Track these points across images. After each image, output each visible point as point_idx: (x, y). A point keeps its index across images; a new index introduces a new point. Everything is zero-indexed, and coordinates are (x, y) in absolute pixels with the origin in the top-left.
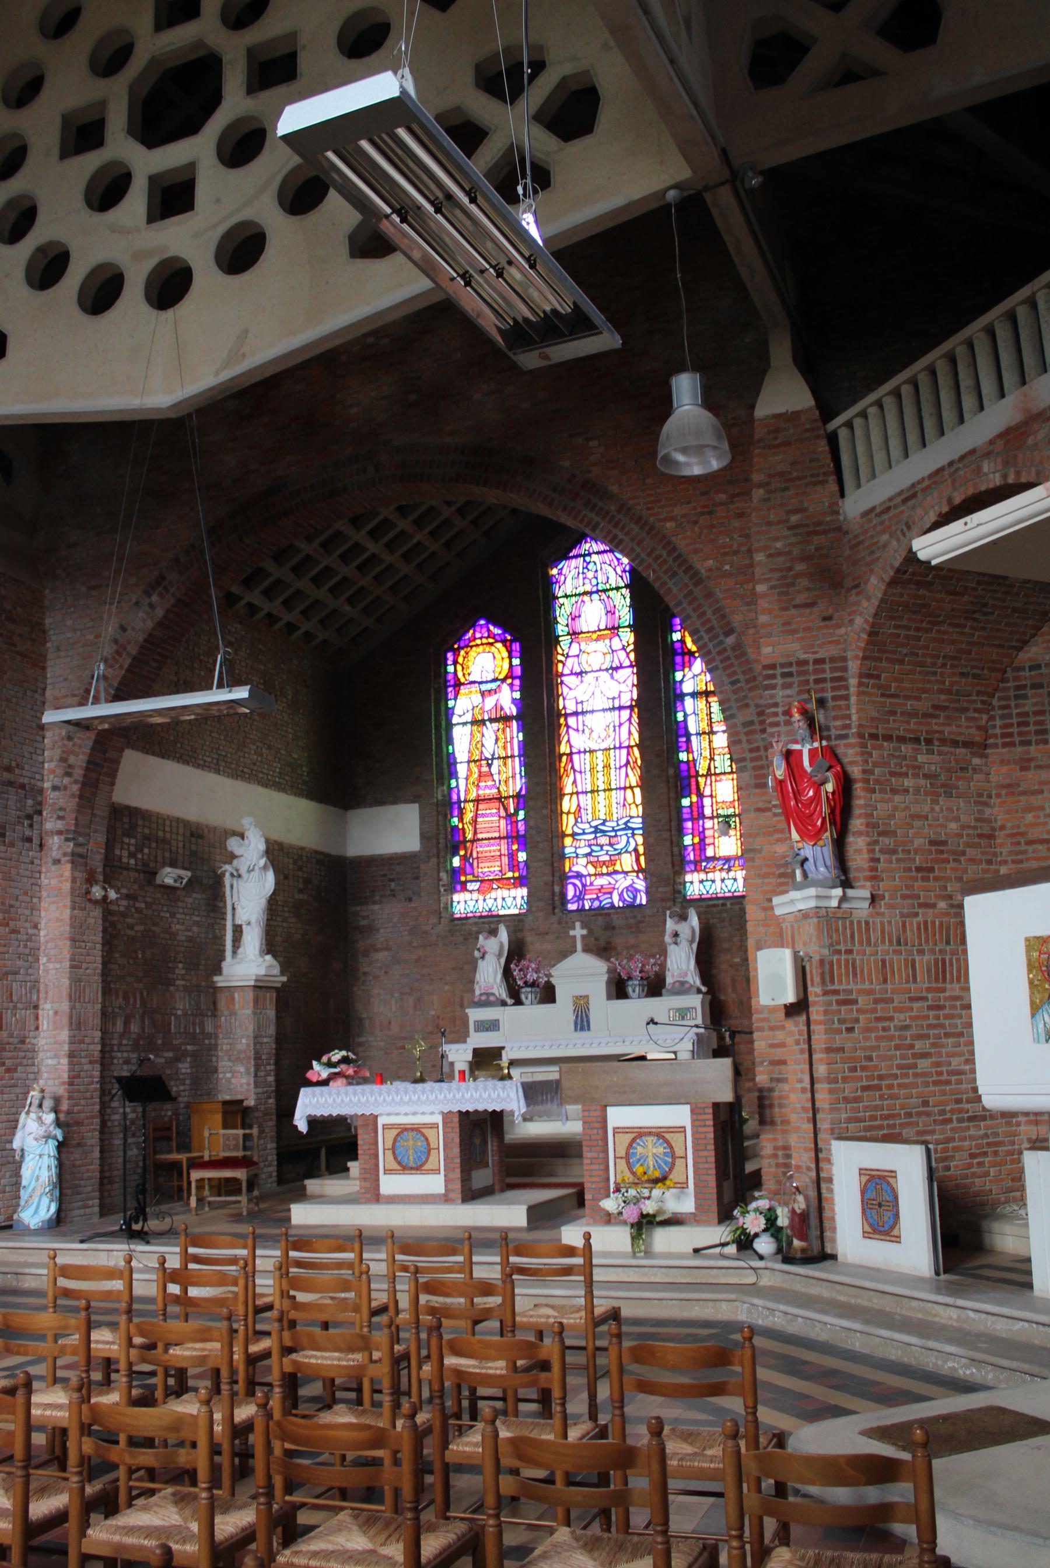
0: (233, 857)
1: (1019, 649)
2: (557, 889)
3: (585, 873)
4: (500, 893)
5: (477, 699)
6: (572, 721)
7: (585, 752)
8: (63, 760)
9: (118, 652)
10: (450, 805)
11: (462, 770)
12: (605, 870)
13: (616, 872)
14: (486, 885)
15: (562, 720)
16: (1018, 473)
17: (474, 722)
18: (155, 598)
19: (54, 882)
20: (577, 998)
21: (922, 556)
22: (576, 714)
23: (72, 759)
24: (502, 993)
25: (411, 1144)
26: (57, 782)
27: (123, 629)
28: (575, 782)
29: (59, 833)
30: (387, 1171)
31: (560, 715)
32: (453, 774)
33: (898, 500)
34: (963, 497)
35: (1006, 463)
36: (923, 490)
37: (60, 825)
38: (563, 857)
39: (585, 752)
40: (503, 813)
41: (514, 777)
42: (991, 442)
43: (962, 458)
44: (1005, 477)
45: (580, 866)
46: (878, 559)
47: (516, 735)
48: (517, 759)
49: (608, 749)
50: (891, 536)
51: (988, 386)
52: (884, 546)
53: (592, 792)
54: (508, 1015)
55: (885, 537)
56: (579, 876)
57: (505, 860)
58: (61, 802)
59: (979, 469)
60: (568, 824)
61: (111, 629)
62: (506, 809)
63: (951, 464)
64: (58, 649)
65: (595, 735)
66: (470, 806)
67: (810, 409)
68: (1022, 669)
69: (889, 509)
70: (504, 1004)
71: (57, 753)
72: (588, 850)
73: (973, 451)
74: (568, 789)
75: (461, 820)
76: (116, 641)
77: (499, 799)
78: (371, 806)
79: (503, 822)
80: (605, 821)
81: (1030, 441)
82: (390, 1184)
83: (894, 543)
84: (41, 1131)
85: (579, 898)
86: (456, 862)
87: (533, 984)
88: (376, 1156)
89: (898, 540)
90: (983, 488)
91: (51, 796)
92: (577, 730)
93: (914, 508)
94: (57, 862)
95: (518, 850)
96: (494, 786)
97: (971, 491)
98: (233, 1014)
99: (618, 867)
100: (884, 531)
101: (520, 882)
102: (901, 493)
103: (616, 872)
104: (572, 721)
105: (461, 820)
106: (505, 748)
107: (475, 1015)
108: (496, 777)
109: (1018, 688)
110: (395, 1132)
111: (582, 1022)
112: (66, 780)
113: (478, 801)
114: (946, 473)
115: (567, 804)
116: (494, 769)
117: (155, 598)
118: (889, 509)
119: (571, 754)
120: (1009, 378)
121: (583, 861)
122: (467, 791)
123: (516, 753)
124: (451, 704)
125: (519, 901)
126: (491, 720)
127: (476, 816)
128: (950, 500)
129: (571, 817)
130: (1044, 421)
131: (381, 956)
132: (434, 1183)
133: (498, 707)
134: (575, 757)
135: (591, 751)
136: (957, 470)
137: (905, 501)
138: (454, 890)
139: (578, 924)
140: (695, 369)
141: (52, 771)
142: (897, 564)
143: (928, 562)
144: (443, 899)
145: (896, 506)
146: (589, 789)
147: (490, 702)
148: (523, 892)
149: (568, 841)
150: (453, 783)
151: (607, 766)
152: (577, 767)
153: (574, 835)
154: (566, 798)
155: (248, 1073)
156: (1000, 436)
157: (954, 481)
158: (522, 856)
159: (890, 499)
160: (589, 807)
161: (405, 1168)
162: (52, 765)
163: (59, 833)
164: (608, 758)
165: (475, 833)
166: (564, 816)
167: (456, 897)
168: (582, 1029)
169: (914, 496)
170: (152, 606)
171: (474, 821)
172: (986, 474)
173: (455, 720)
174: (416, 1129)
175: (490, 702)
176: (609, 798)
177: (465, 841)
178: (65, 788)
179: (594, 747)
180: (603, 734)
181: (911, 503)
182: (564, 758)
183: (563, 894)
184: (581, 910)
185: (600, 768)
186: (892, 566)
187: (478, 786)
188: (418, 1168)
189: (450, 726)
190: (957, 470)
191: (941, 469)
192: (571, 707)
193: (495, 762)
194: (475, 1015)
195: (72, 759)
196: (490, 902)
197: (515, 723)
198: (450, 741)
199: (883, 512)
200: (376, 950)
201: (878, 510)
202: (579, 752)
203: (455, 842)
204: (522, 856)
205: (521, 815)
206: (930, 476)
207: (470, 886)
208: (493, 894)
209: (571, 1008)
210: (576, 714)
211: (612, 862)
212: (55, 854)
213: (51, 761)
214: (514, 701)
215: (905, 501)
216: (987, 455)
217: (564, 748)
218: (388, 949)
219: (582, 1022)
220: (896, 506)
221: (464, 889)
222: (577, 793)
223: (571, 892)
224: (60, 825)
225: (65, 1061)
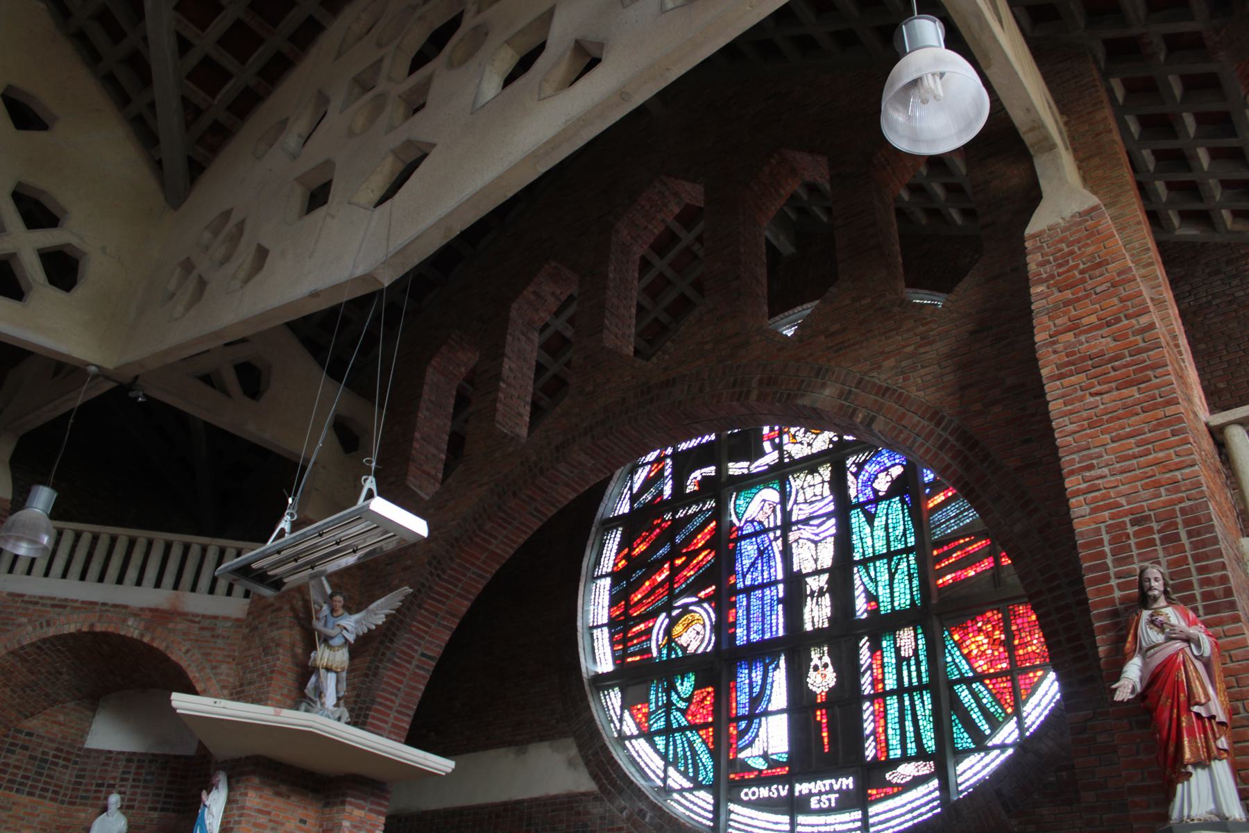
1: (27, 717)
16: (153, 639)
21: (174, 704)
33: (49, 602)
34: (103, 630)
35: (147, 628)
36: (73, 608)
42: (142, 609)
43: (115, 606)
44: (142, 635)
46: (8, 631)
50: (29, 621)
51: (151, 573)
52: (20, 625)
55: (24, 620)
59: (125, 620)
63: (104, 604)
67: (7, 500)
68: (20, 731)
69: (36, 603)
73: (126, 607)
81: (171, 626)
83: (30, 628)
89: (35, 628)
90: (122, 633)
93: (59, 614)
97: (111, 629)
100: (25, 615)
102: (54, 599)
109: (12, 744)
114: (98, 608)
118: (36, 603)
120: (169, 579)
128: (92, 625)
130: (184, 620)
136: (107, 611)
137: (54, 606)
140: (54, 487)
142: (25, 643)
143: (174, 710)
145: (43, 605)
156: (151, 610)
157: (101, 616)
159: (42, 598)
169: (64, 607)
172: (128, 626)
181: (57, 610)
186: (19, 642)
190: (107, 611)
191: (94, 603)
199: (30, 602)
201: (26, 599)
206: (83, 602)
215: (54, 606)
216: (135, 615)
220: (43, 605)
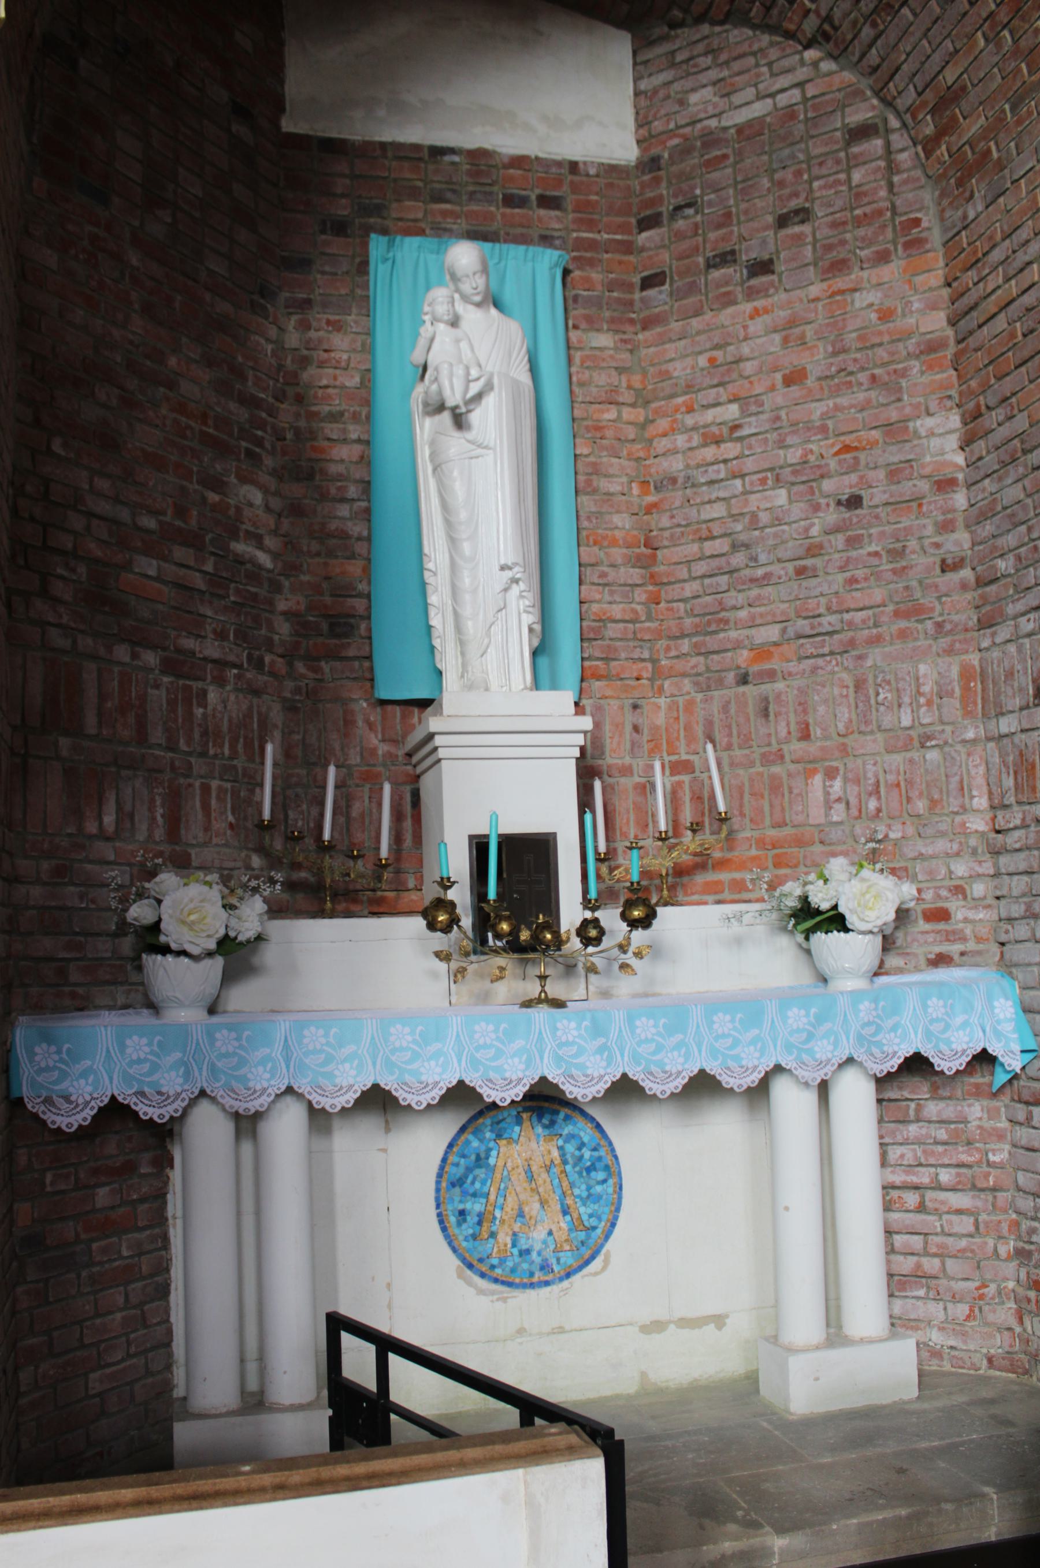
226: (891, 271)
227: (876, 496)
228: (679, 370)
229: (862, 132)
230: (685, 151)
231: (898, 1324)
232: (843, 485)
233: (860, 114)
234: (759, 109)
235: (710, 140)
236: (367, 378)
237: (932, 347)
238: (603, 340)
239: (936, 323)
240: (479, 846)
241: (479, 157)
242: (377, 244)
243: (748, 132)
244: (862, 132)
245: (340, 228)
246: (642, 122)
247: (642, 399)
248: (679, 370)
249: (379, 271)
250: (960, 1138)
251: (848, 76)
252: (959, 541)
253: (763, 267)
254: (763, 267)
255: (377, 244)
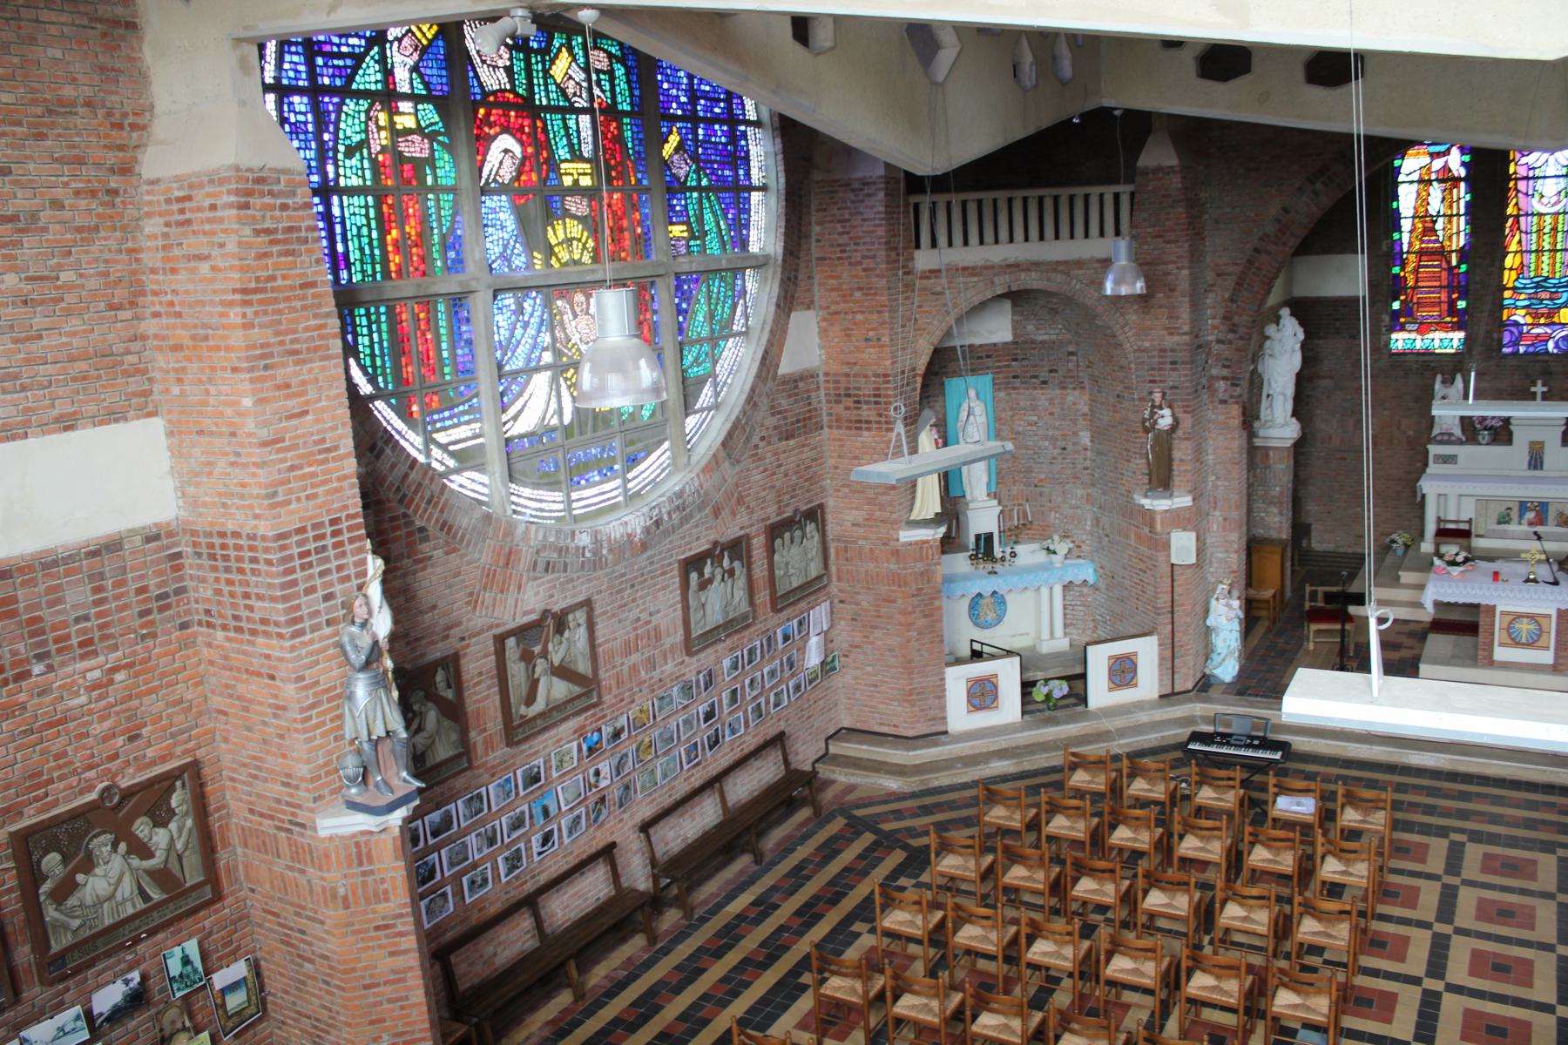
0: (1268, 338)
2: (1495, 336)
3: (1522, 321)
4: (1438, 335)
5: (1426, 160)
6: (1522, 185)
7: (1533, 215)
8: (1226, 318)
9: (1280, 231)
10: (1399, 259)
11: (1406, 225)
12: (1542, 321)
13: (1554, 324)
14: (1423, 329)
15: (1511, 184)
17: (1420, 181)
18: (1319, 186)
19: (1221, 418)
20: (1532, 443)
22: (1527, 178)
23: (1236, 319)
24: (1457, 432)
25: (1525, 627)
26: (1221, 336)
27: (1286, 210)
28: (1520, 242)
29: (1225, 378)
30: (1501, 645)
31: (1509, 179)
32: (1398, 228)
37: (1225, 372)
38: (1502, 307)
39: (1533, 215)
40: (1444, 265)
41: (1458, 233)
45: (1520, 316)
47: (1462, 193)
48: (1463, 219)
49: (1558, 214)
53: (1537, 251)
54: (1464, 452)
56: (1516, 324)
57: (1445, 307)
58: (1227, 354)
60: (1509, 278)
61: (1274, 209)
62: (1449, 262)
64: (1217, 222)
65: (1545, 200)
66: (1412, 258)
70: (1461, 443)
71: (1221, 312)
72: (1526, 303)
74: (1513, 247)
75: (1403, 269)
76: (1278, 221)
77: (1441, 253)
78: (1317, 253)
79: (1444, 274)
80: (1547, 278)
82: (1501, 654)
84: (1232, 614)
85: (1516, 343)
86: (1396, 305)
87: (1491, 428)
88: (1492, 634)
91: (1216, 348)
92: (1526, 194)
94: (1224, 402)
95: (1458, 299)
96: (1437, 241)
98: (1267, 467)
99: (1555, 320)
101: (1456, 327)
103: (1554, 324)
104: (1522, 185)
105: (1403, 269)
106: (1451, 207)
107: (1433, 450)
108: (1440, 233)
110: (1510, 617)
111: (1536, 461)
112: (1230, 336)
113: (1421, 253)
115: (1509, 261)
116: (1439, 225)
117: (1319, 186)
119: (1517, 217)
121: (1523, 312)
122: (1411, 244)
123: (1462, 211)
124: (1397, 163)
125: (1456, 343)
126: (1439, 181)
127: (1419, 266)
129: (1514, 274)
131: (1324, 383)
132: (1547, 657)
133: (1446, 169)
134: (1522, 219)
135: (1540, 215)
138: (1392, 329)
139: (1539, 383)
141: (1214, 327)
144: (1384, 338)
146: (1534, 247)
147: (1438, 164)
148: (1462, 335)
149: (1507, 294)
150: (1396, 236)
151: (1554, 229)
152: (1523, 228)
153: (1514, 288)
154: (1510, 257)
155: (1281, 513)
158: (1462, 304)
160: (1533, 266)
161: (1517, 643)
162: (1216, 322)
163: (1225, 378)
164: (1556, 221)
165: (1417, 281)
166: (1506, 273)
167: (1394, 336)
168: (1535, 468)
170: (1315, 193)
171: (1416, 271)
173: (1401, 178)
174: (1532, 617)
175: (1438, 164)
176: (1554, 258)
177: (1405, 288)
178: (1230, 342)
179: (1543, 210)
180: (1554, 200)
182: (1510, 221)
183: (1500, 340)
184: (1516, 353)
185: (1547, 230)
187: (1422, 242)
188: (1530, 645)
189: (1396, 184)
192: (1522, 172)
193: (1441, 220)
194: (1433, 450)
195: (1236, 319)
196: (1427, 342)
197: (1463, 185)
198: (1396, 197)
200: (1319, 377)
202: (1527, 215)
203: (1398, 285)
204: (1462, 304)
205: (1463, 268)
207: (1408, 327)
208: (1431, 335)
209: (1526, 450)
210: (1527, 178)
211: (1550, 315)
212: (1221, 395)
213: (1214, 318)
214: (1463, 164)
217: (1510, 210)
218: (1330, 377)
219: (1536, 461)
221: (1402, 328)
222: (1522, 252)
223: (1506, 338)
224: (1225, 372)
225: (1234, 556)
226: (1077, 392)
227: (1070, 447)
228: (1022, 404)
229: (1071, 354)
230: (1025, 342)
231: (1066, 634)
232: (1060, 444)
233: (1071, 349)
234: (1046, 337)
235: (1033, 342)
236: (945, 415)
237: (1084, 415)
238: (1002, 394)
239: (1086, 409)
240: (978, 537)
241: (971, 346)
242: (946, 381)
243: (1043, 342)
244: (1071, 354)
245: (936, 374)
246: (1014, 329)
247: (1012, 409)
248: (1022, 404)
249: (947, 387)
250: (1082, 595)
251: (1069, 336)
252: (1088, 463)
253: (1045, 382)
254: (1045, 382)
255: (946, 381)
